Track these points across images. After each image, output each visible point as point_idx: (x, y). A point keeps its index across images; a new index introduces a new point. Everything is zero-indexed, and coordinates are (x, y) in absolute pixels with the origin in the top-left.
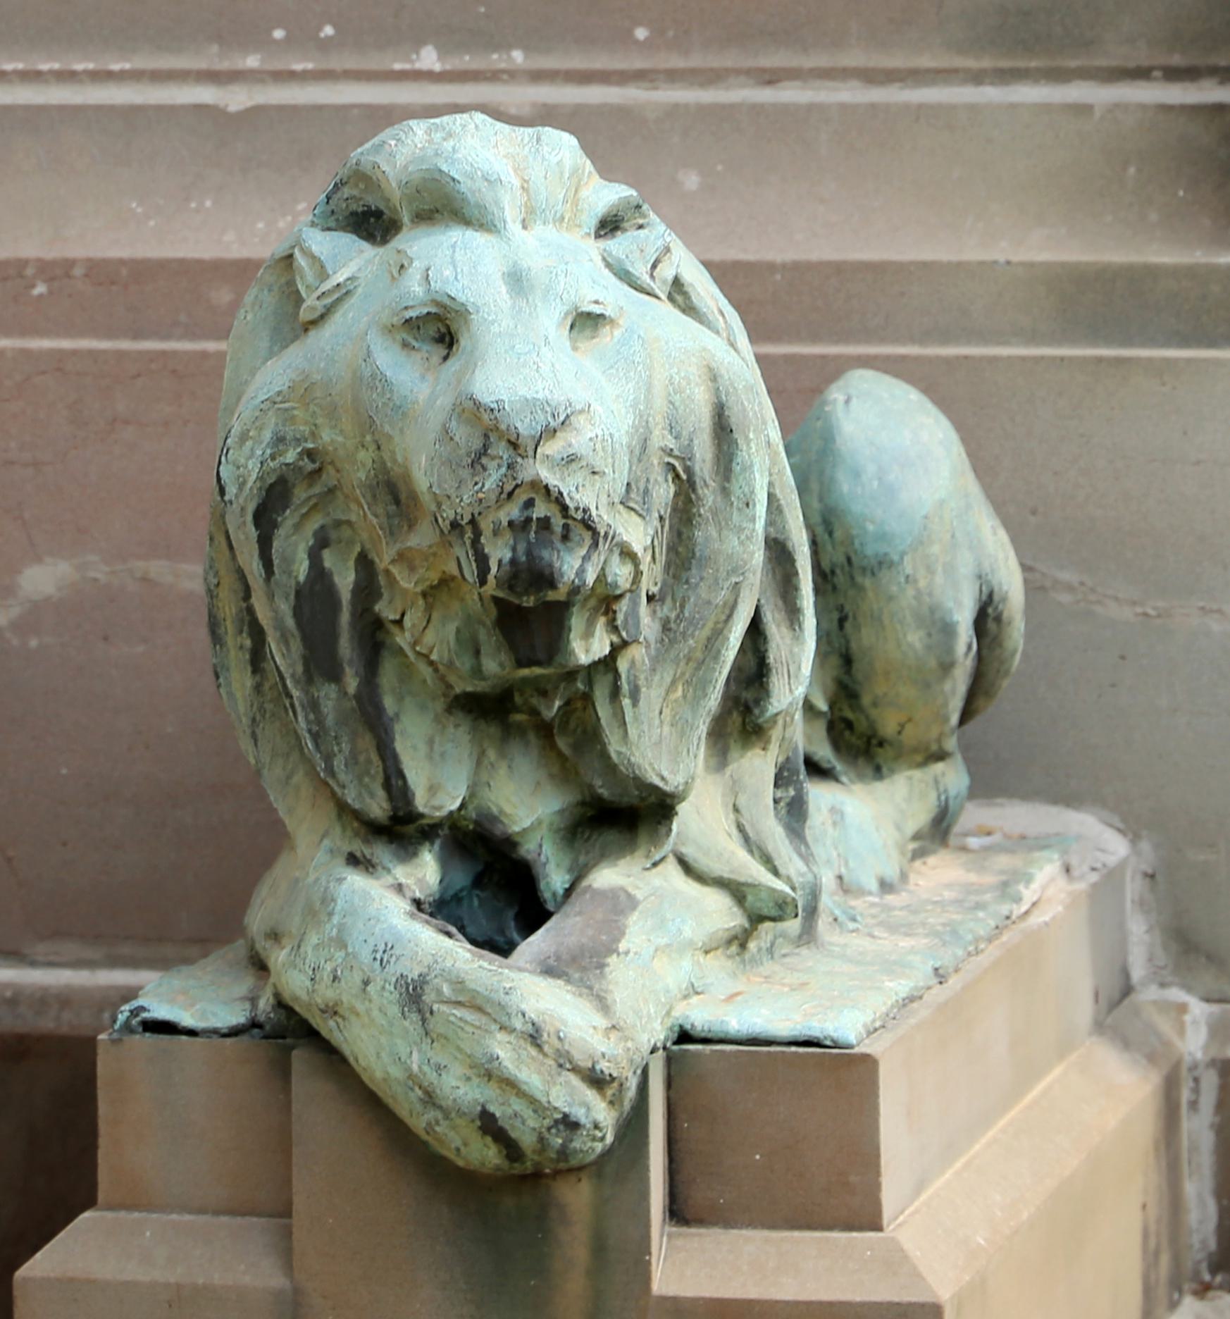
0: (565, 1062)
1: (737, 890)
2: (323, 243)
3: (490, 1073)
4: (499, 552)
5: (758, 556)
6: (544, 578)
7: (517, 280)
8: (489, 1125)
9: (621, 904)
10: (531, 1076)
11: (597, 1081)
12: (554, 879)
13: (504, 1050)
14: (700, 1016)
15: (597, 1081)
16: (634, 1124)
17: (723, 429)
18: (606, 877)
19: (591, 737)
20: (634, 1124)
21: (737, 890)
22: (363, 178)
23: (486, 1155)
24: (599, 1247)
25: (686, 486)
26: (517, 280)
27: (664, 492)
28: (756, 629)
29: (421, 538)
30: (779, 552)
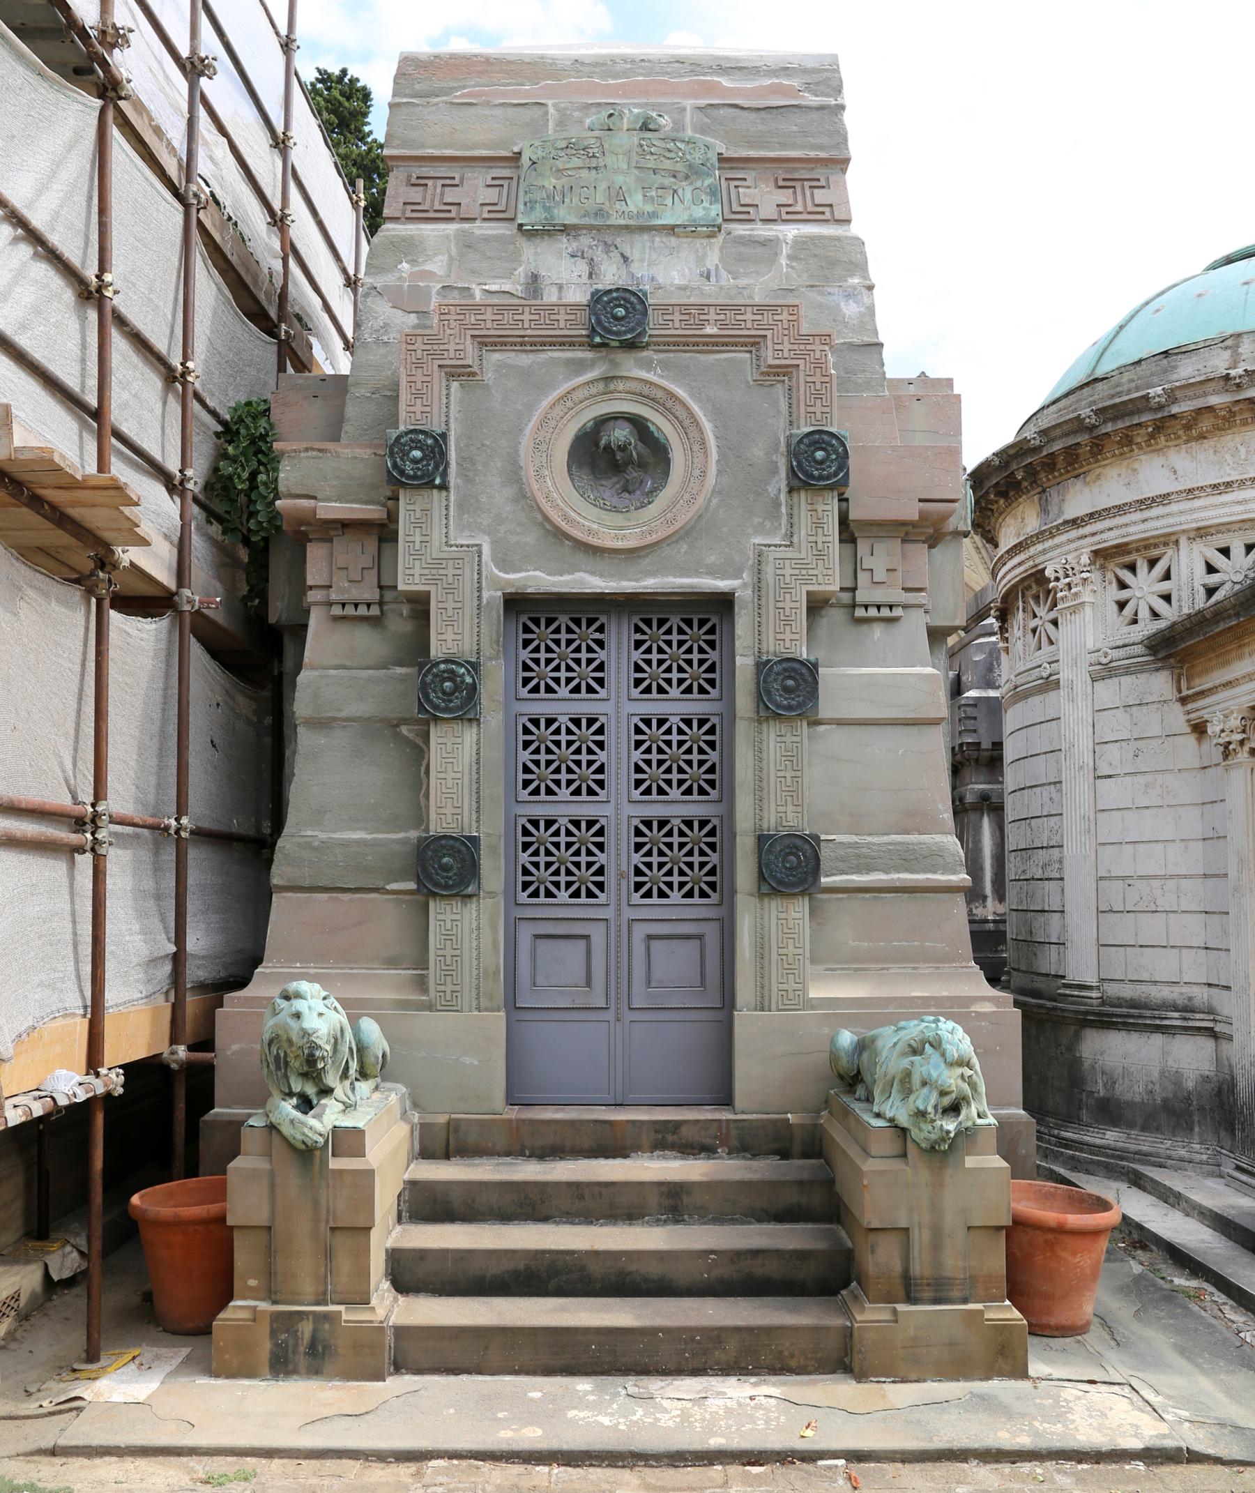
0: (316, 1132)
1: (344, 1103)
2: (279, 1001)
3: (304, 1134)
4: (306, 1052)
5: (347, 1050)
6: (313, 1055)
7: (310, 1008)
8: (303, 1142)
9: (325, 1106)
10: (310, 1135)
11: (321, 1135)
12: (315, 1102)
13: (306, 1131)
14: (337, 1124)
15: (321, 1135)
16: (327, 1142)
17: (342, 1031)
18: (323, 1102)
19: (321, 1079)
20: (327, 1142)
21: (344, 1103)
22: (285, 990)
23: (303, 1147)
24: (321, 1161)
25: (336, 1040)
26: (310, 1008)
27: (333, 1041)
28: (347, 1062)
29: (294, 1049)
30: (351, 1049)
